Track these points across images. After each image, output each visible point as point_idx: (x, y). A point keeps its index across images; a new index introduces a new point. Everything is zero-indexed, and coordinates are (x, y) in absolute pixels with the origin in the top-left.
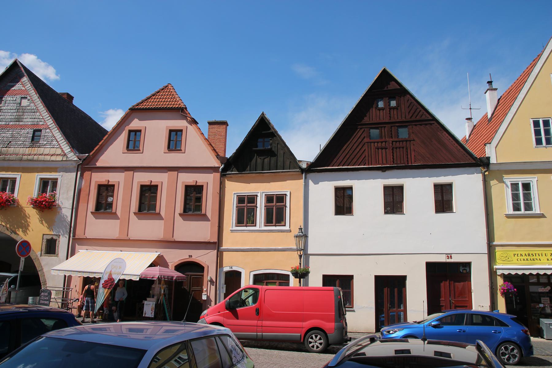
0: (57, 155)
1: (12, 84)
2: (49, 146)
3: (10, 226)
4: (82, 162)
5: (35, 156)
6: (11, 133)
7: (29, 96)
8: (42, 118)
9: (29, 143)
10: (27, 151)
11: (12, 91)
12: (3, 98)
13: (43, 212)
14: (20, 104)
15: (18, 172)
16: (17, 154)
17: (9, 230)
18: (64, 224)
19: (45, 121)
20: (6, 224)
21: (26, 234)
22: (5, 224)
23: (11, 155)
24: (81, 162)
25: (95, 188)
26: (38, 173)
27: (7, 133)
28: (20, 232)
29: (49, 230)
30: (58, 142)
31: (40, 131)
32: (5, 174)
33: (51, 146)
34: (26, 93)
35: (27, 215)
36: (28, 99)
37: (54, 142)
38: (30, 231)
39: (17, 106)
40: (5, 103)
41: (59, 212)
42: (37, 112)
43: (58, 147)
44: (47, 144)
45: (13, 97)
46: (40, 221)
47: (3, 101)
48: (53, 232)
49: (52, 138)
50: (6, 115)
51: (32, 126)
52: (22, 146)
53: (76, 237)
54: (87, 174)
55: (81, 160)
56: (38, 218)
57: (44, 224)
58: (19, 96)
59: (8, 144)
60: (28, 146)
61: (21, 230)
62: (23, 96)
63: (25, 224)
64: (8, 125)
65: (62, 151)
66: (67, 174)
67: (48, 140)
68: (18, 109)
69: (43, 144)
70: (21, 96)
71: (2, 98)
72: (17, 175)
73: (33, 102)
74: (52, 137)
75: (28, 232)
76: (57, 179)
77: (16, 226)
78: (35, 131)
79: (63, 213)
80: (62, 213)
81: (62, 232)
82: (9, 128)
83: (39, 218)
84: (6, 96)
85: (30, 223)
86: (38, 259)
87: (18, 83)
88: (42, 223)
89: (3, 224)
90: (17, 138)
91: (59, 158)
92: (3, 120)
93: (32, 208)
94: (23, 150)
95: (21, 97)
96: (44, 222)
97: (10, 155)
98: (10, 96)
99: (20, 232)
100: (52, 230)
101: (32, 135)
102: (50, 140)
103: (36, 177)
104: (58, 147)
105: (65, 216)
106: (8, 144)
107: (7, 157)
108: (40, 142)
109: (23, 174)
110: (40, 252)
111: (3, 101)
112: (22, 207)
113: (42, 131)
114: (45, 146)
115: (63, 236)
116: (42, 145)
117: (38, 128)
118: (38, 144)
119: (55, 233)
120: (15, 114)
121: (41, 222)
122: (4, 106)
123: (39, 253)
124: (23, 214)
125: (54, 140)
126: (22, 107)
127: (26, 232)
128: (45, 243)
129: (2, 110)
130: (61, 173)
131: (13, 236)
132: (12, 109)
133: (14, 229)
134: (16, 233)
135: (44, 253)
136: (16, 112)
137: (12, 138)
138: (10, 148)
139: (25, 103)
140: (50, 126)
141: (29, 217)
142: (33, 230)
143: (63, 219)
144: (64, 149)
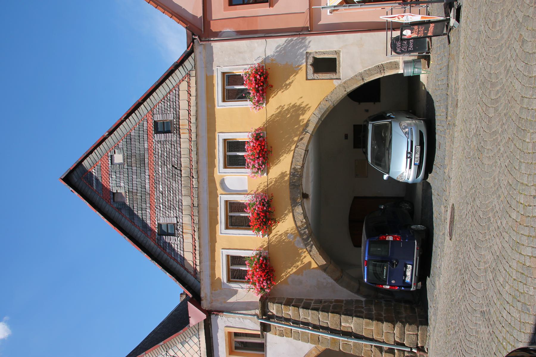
0: (189, 86)
1: (94, 182)
2: (177, 103)
3: (296, 136)
4: (195, 36)
5: (191, 121)
6: (160, 169)
7: (109, 154)
8: (138, 126)
9: (173, 136)
10: (184, 136)
11: (104, 181)
12: (114, 192)
13: (272, 86)
14: (120, 164)
15: (215, 139)
16: (190, 150)
17: (302, 136)
18: (289, 48)
19: (143, 120)
20: (293, 142)
21: (308, 107)
22: (294, 144)
23: (191, 159)
24: (197, 37)
25: (236, 10)
26: (214, 106)
27: (160, 175)
28: (305, 117)
29: (300, 71)
30: (171, 91)
31: (156, 123)
32: (218, 158)
33: (177, 99)
34: (105, 159)
35: (279, 110)
36: (113, 153)
37: (171, 96)
38: (303, 102)
39: (124, 168)
40: (120, 187)
41: (272, 60)
42: (131, 135)
43: (177, 89)
44: (175, 107)
45: (112, 177)
46: (286, 89)
47: (117, 191)
48: (302, 63)
49: (166, 102)
50: (136, 182)
51: (150, 137)
52: (178, 145)
53: (309, 26)
54: (214, 27)
55: (194, 39)
56: (282, 92)
57: (290, 81)
58: (110, 168)
59: (176, 168)
60: (178, 136)
61: (301, 117)
62: (110, 163)
63: (293, 111)
64: (149, 175)
65: (183, 81)
66: (215, 59)
67: (169, 107)
68: (128, 166)
69: (174, 114)
70: (110, 165)
71: (114, 193)
72: (220, 138)
73: (117, 146)
74: (164, 102)
75: (303, 105)
76: (223, 74)
77: (296, 127)
78: (157, 132)
79: (272, 53)
80: (274, 56)
81: (301, 51)
82: (153, 173)
83: (283, 90)
84: (111, 188)
85: (290, 104)
86: (345, 83)
87: (93, 174)
88: (290, 84)
89: (293, 147)
90: (167, 157)
91: (193, 80)
92: (143, 185)
93: (267, 105)
94: (184, 142)
95: (112, 164)
96: (287, 82)
97: (191, 161)
98: (111, 182)
99: (305, 117)
100: (300, 66)
101: (163, 135)
102: (169, 103)
103: (221, 108)
104: (177, 89)
105: (278, 49)
106: (176, 168)
107: (195, 166)
108: (172, 119)
109: (218, 130)
110: (334, 81)
111: (117, 191)
112: (267, 121)
113: (156, 120)
114: (178, 109)
115: (307, 47)
116: (176, 115)
117: (152, 128)
118: (175, 120)
119: (304, 61)
120: (134, 168)
121: (288, 87)
122: (125, 187)
123: (336, 83)
124: (277, 118)
125: (169, 98)
126: (124, 160)
127: (304, 108)
128: (320, 75)
129: (130, 190)
130: (215, 68)
131: (311, 128)
132: (128, 174)
133: (301, 129)
134: (307, 125)
135: (334, 74)
136: (131, 168)
137: (168, 165)
138: (181, 164)
139: (118, 158)
140: (149, 109)
141: (281, 108)
142: (301, 97)
143: (282, 52)
144: (181, 78)
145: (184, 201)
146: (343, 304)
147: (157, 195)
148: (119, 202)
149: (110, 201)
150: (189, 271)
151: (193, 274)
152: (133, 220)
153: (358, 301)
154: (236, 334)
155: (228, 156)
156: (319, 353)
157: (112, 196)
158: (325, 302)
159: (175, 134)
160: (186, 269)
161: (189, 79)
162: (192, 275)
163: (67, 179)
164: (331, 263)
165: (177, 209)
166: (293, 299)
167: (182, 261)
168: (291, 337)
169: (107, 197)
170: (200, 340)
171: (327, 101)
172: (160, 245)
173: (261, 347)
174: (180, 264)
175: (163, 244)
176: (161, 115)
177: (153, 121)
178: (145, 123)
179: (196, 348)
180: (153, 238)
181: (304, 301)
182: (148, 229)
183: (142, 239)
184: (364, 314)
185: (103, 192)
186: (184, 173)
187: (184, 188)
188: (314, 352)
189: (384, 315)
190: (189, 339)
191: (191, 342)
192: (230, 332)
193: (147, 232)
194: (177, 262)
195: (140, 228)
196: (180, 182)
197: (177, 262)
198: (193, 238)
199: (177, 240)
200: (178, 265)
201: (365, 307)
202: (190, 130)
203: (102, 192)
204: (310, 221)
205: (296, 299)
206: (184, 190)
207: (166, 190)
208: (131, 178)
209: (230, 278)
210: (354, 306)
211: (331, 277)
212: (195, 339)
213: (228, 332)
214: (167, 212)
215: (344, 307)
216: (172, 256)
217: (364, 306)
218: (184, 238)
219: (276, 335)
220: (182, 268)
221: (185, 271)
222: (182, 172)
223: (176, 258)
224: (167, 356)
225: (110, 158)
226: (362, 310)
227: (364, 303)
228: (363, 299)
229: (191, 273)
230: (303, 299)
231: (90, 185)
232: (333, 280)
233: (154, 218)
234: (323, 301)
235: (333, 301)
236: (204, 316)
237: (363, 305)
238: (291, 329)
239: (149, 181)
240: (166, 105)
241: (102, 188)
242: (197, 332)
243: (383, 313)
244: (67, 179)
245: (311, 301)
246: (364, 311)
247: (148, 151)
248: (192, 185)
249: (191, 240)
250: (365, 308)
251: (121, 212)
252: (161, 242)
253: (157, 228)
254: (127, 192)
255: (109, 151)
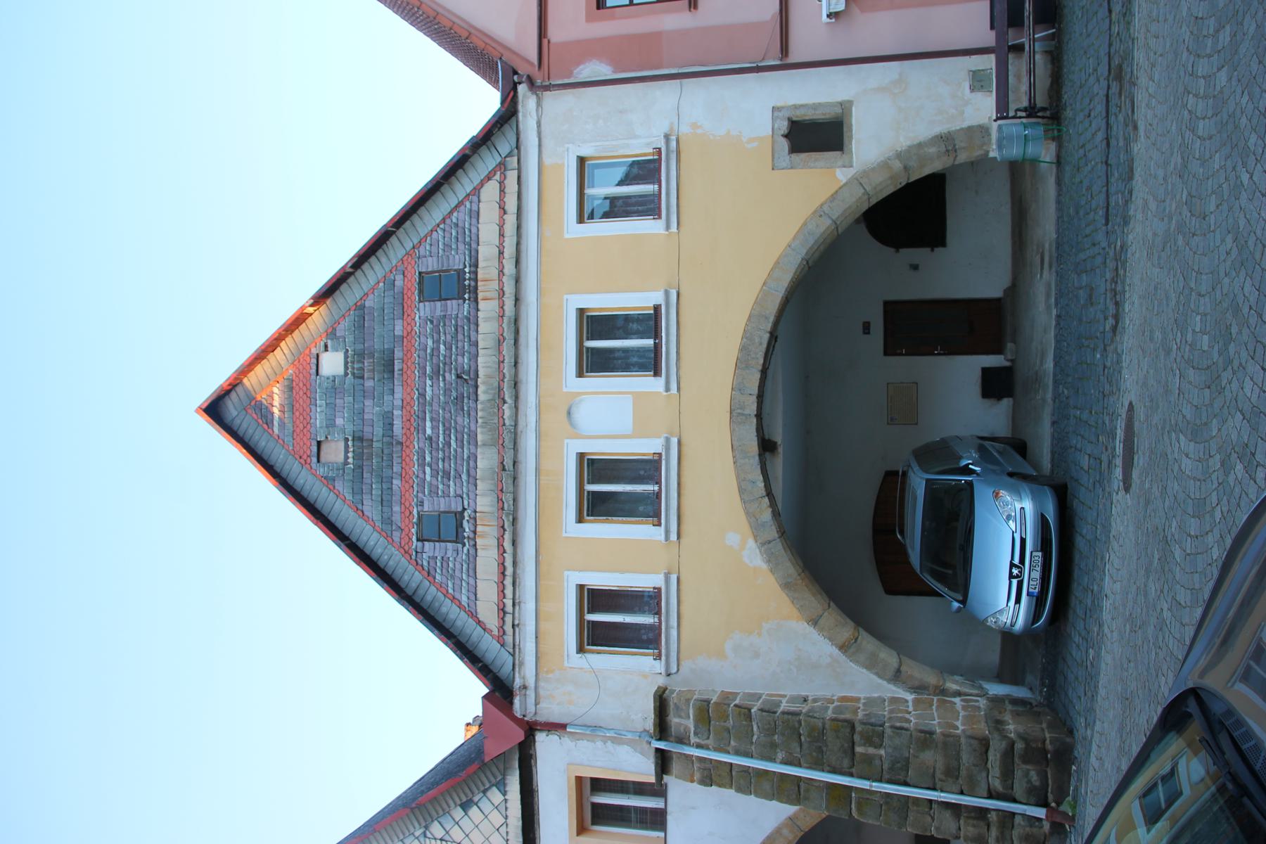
0: (502, 191)
10: (487, 308)
16: (500, 342)
36: (322, 348)
62: (314, 371)
94: (487, 320)
107: (510, 374)
114: (474, 246)
125: (454, 220)
137: (447, 375)
145: (483, 458)
146: (861, 705)
147: (418, 444)
148: (330, 463)
149: (309, 461)
150: (488, 626)
151: (496, 633)
152: (360, 506)
153: (894, 700)
154: (599, 785)
155: (588, 349)
156: (800, 834)
157: (315, 449)
158: (815, 701)
159: (467, 301)
160: (479, 622)
161: (502, 175)
162: (493, 637)
163: (214, 410)
164: (829, 606)
165: (464, 477)
166: (737, 694)
167: (472, 604)
168: (731, 787)
169: (304, 452)
170: (506, 797)
171: (821, 216)
172: (422, 566)
173: (656, 820)
174: (467, 609)
175: (429, 562)
176: (435, 259)
177: (417, 274)
178: (399, 278)
179: (497, 818)
180: (407, 548)
181: (764, 697)
182: (394, 528)
183: (380, 551)
184: (912, 724)
185: (294, 439)
186: (485, 392)
187: (482, 427)
188: (785, 832)
189: (961, 728)
190: (481, 795)
191: (485, 804)
192: (581, 777)
193: (392, 534)
194: (460, 606)
195: (377, 524)
196: (473, 413)
197: (460, 606)
198: (500, 546)
199: (460, 552)
200: (463, 613)
201: (914, 710)
202: (502, 293)
203: (291, 439)
204: (780, 509)
205: (744, 693)
206: (482, 433)
207: (441, 432)
208: (362, 405)
209: (586, 644)
210: (887, 709)
211: (830, 639)
212: (496, 796)
213: (576, 777)
214: (441, 486)
215: (863, 710)
216: (447, 591)
217: (911, 709)
218: (478, 547)
219: (692, 781)
220: (470, 620)
221: (478, 627)
222: (479, 390)
223: (457, 595)
224: (427, 840)
225: (314, 361)
226: (907, 716)
227: (910, 704)
228: (910, 697)
229: (492, 631)
230: (760, 696)
231: (267, 424)
232: (834, 647)
233: (411, 499)
234: (810, 698)
235: (835, 698)
236: (520, 735)
237: (908, 707)
238: (731, 764)
239: (402, 411)
240: (447, 235)
241: (294, 431)
242: (500, 777)
243: (959, 724)
244: (214, 410)
245: (781, 699)
246: (912, 719)
247: (403, 342)
248: (501, 419)
249: (494, 553)
250: (913, 713)
251: (334, 487)
252: (424, 557)
253: (417, 525)
254: (350, 438)
255: (314, 344)
